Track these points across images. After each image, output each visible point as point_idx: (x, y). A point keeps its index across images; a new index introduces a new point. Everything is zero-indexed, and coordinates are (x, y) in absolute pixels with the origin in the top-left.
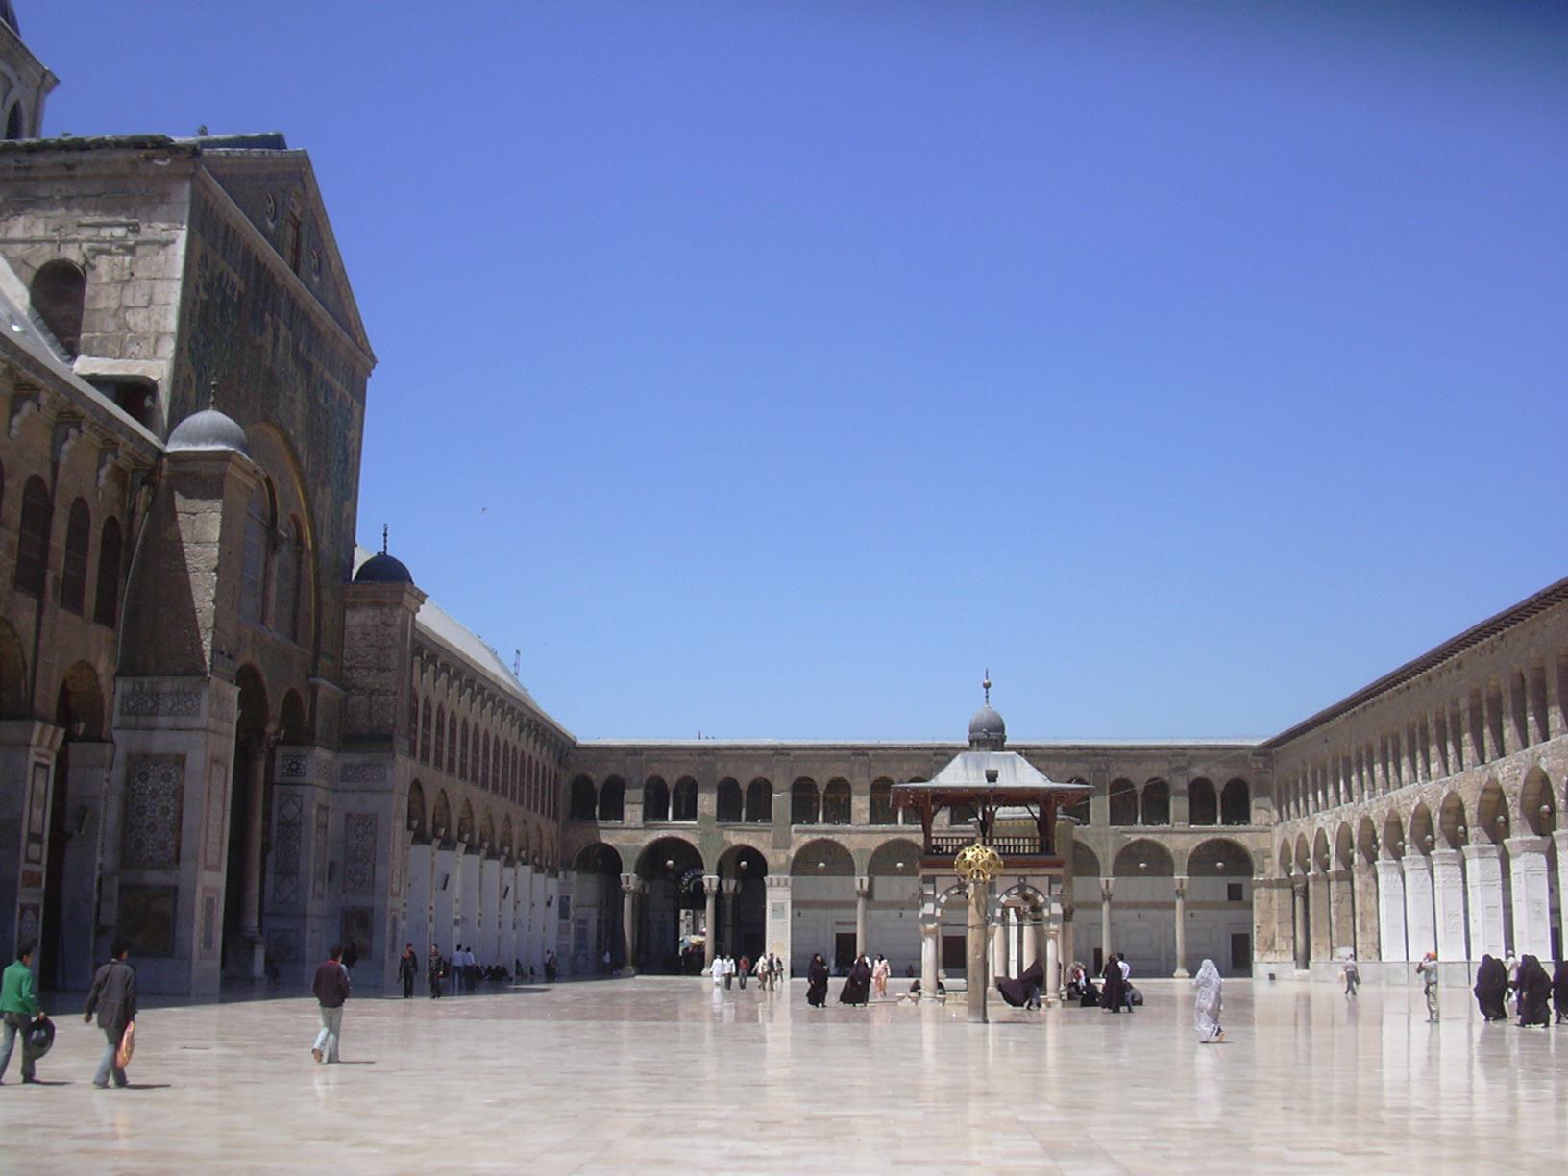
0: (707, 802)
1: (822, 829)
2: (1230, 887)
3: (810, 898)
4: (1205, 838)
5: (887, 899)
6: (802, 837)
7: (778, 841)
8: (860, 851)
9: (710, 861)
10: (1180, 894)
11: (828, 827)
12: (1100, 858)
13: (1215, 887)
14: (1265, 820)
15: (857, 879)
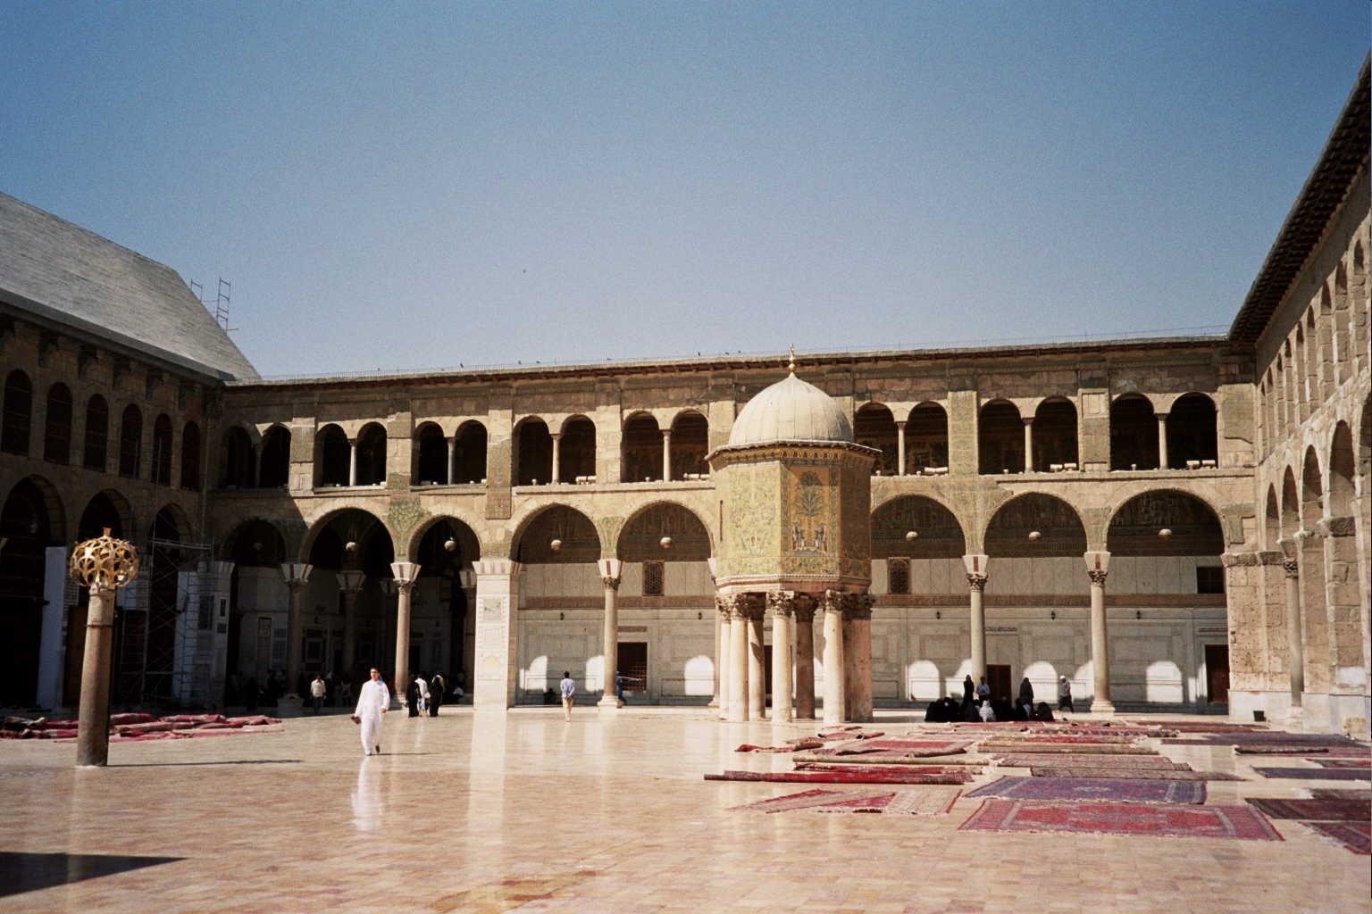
0: (399, 456)
1: (553, 493)
2: (1202, 572)
3: (575, 593)
4: (1135, 489)
5: (680, 593)
6: (529, 502)
7: (492, 511)
8: (607, 520)
9: (402, 543)
10: (1098, 577)
11: (565, 487)
12: (963, 524)
13: (1179, 573)
14: (1244, 458)
15: (602, 563)
